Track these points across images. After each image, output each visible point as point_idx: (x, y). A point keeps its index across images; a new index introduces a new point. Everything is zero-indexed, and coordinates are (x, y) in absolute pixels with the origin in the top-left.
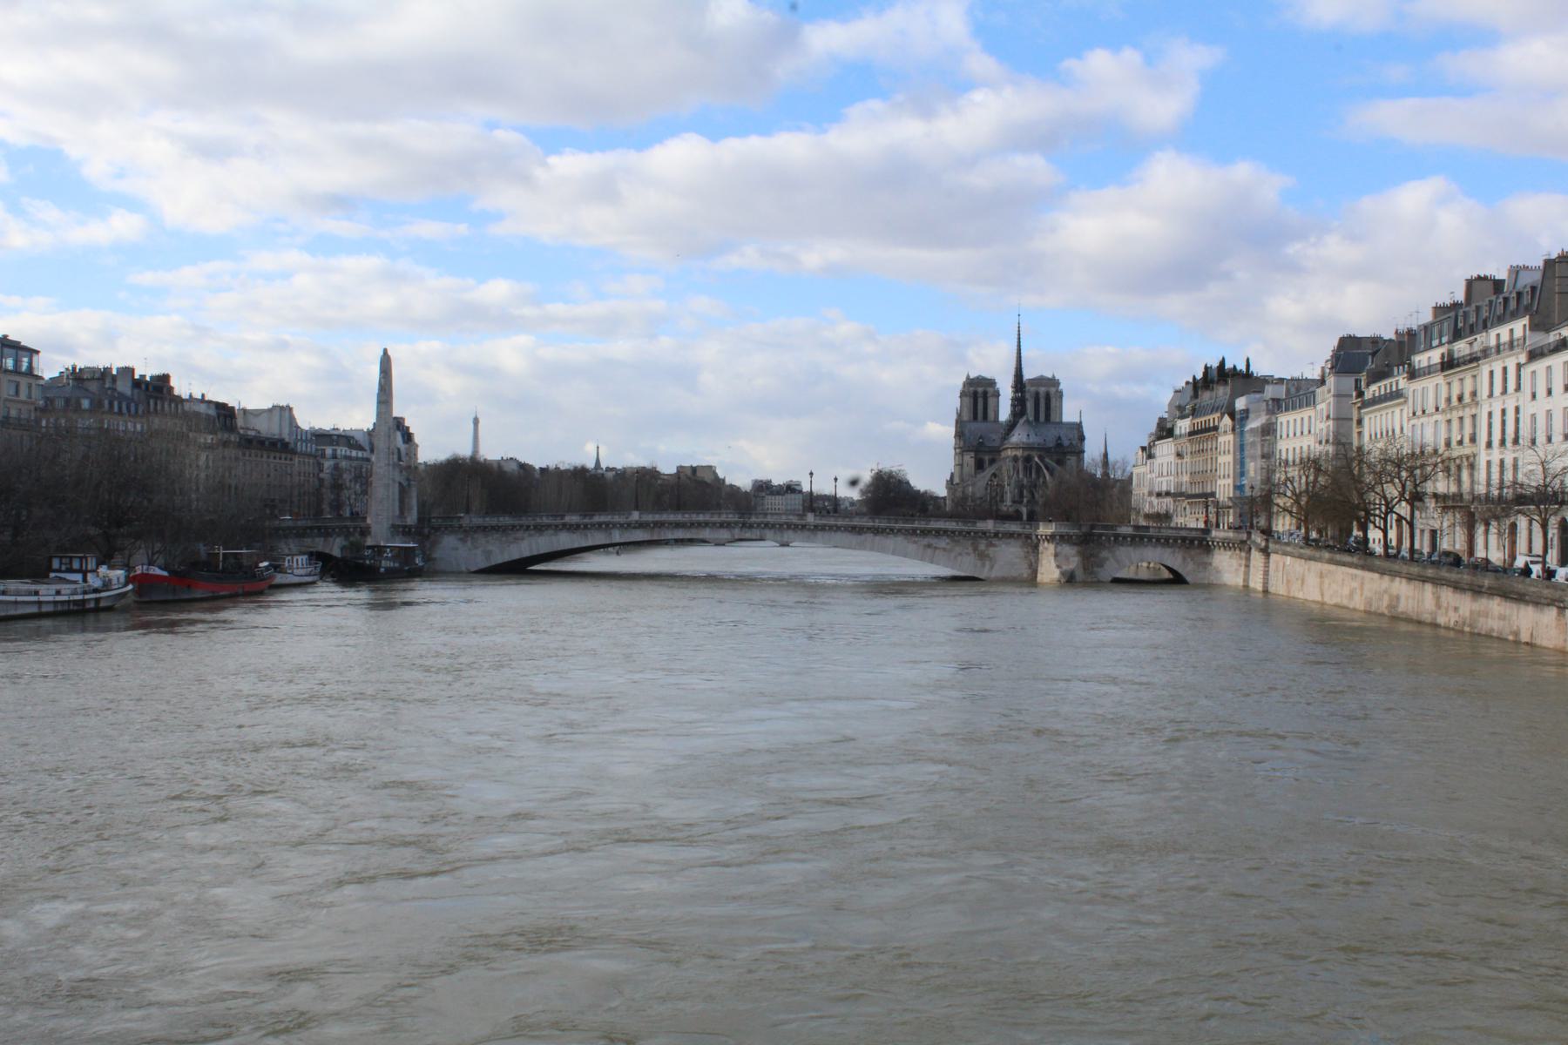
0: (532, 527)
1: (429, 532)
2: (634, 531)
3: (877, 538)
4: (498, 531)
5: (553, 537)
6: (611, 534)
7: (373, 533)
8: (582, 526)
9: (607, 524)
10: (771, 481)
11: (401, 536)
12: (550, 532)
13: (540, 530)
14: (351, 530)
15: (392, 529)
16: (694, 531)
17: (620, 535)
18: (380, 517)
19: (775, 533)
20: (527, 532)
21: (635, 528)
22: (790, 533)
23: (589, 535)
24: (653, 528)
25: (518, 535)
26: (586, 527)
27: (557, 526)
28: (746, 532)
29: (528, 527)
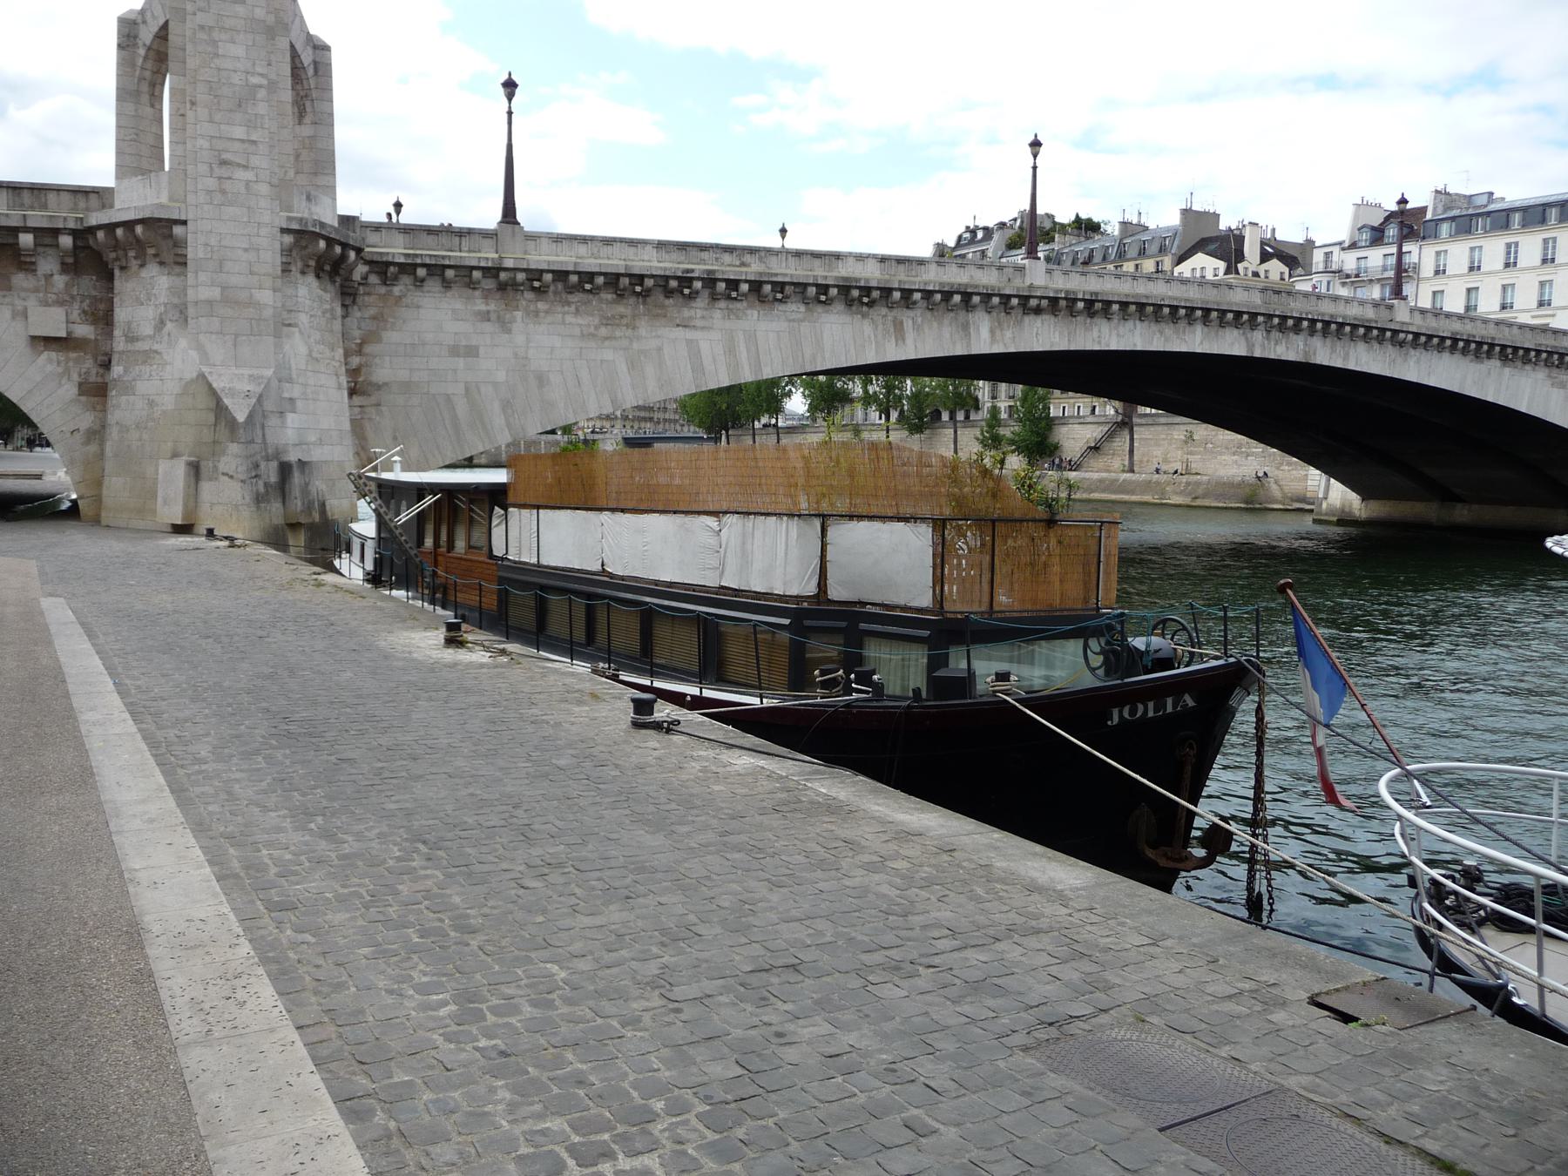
0: (745, 287)
1: (365, 278)
2: (1027, 319)
3: (1507, 370)
4: (620, 295)
5: (805, 328)
6: (965, 327)
7: (194, 252)
8: (897, 295)
9: (967, 296)
10: (1216, 216)
11: (311, 279)
12: (795, 309)
13: (762, 299)
14: (26, 239)
15: (288, 239)
16: (1168, 329)
17: (992, 332)
18: (241, 175)
19: (1333, 351)
20: (722, 304)
21: (1038, 311)
22: (1361, 346)
23: (908, 324)
24: (1080, 312)
25: (686, 313)
26: (907, 293)
27: (823, 289)
28: (1276, 344)
29: (733, 284)
